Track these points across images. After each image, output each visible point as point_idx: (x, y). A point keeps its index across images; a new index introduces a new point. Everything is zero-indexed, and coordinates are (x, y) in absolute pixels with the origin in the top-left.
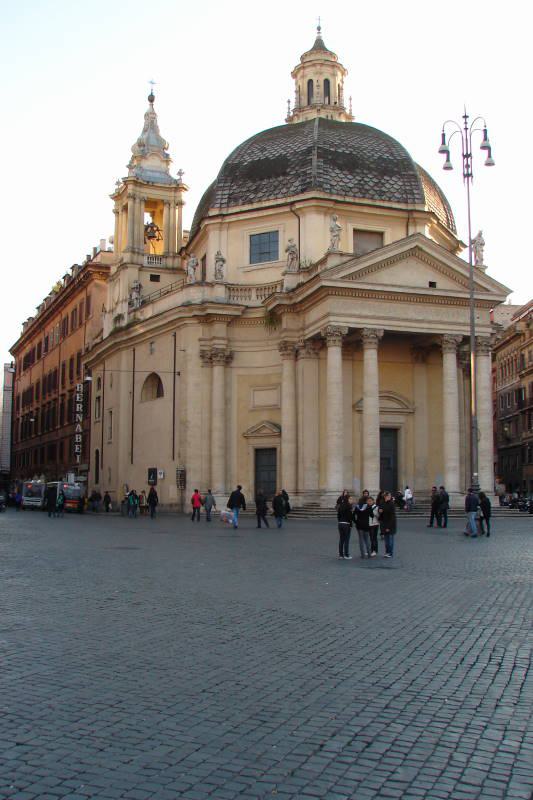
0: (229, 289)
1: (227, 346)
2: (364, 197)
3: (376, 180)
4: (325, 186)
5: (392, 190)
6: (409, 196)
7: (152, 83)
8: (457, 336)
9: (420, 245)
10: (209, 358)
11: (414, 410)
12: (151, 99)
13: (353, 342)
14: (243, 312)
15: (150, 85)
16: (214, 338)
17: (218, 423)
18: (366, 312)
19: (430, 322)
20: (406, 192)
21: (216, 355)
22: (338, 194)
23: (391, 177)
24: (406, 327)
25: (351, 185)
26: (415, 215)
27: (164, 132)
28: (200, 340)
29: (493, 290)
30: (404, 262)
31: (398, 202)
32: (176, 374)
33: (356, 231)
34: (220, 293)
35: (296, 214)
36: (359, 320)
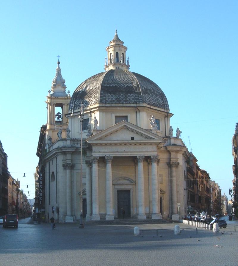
0: (73, 141)
1: (71, 162)
2: (119, 103)
3: (124, 96)
4: (103, 101)
5: (131, 99)
6: (137, 101)
7: (59, 57)
8: (142, 156)
9: (126, 125)
10: (65, 166)
11: (136, 183)
12: (59, 63)
13: (102, 160)
14: (76, 150)
15: (58, 58)
16: (66, 160)
17: (68, 190)
18: (106, 151)
19: (131, 152)
20: (136, 99)
21: (67, 166)
22: (109, 103)
23: (131, 94)
24: (122, 155)
25: (114, 99)
26: (139, 108)
27: (64, 76)
28: (63, 160)
29: (156, 138)
31: (133, 103)
32: (57, 172)
33: (116, 117)
34: (68, 143)
36: (103, 154)
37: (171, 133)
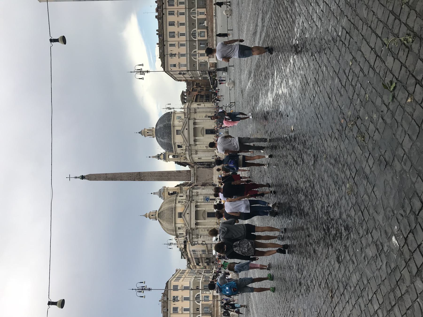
7: (147, 157)
10: (196, 154)
12: (150, 157)
30: (184, 134)
35: (175, 143)
37: (183, 112)
